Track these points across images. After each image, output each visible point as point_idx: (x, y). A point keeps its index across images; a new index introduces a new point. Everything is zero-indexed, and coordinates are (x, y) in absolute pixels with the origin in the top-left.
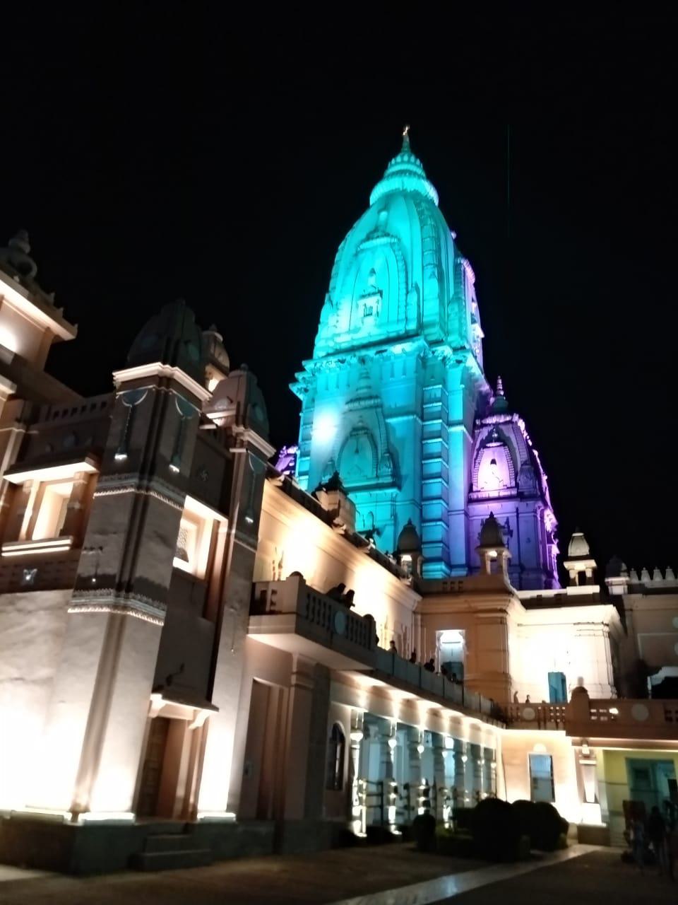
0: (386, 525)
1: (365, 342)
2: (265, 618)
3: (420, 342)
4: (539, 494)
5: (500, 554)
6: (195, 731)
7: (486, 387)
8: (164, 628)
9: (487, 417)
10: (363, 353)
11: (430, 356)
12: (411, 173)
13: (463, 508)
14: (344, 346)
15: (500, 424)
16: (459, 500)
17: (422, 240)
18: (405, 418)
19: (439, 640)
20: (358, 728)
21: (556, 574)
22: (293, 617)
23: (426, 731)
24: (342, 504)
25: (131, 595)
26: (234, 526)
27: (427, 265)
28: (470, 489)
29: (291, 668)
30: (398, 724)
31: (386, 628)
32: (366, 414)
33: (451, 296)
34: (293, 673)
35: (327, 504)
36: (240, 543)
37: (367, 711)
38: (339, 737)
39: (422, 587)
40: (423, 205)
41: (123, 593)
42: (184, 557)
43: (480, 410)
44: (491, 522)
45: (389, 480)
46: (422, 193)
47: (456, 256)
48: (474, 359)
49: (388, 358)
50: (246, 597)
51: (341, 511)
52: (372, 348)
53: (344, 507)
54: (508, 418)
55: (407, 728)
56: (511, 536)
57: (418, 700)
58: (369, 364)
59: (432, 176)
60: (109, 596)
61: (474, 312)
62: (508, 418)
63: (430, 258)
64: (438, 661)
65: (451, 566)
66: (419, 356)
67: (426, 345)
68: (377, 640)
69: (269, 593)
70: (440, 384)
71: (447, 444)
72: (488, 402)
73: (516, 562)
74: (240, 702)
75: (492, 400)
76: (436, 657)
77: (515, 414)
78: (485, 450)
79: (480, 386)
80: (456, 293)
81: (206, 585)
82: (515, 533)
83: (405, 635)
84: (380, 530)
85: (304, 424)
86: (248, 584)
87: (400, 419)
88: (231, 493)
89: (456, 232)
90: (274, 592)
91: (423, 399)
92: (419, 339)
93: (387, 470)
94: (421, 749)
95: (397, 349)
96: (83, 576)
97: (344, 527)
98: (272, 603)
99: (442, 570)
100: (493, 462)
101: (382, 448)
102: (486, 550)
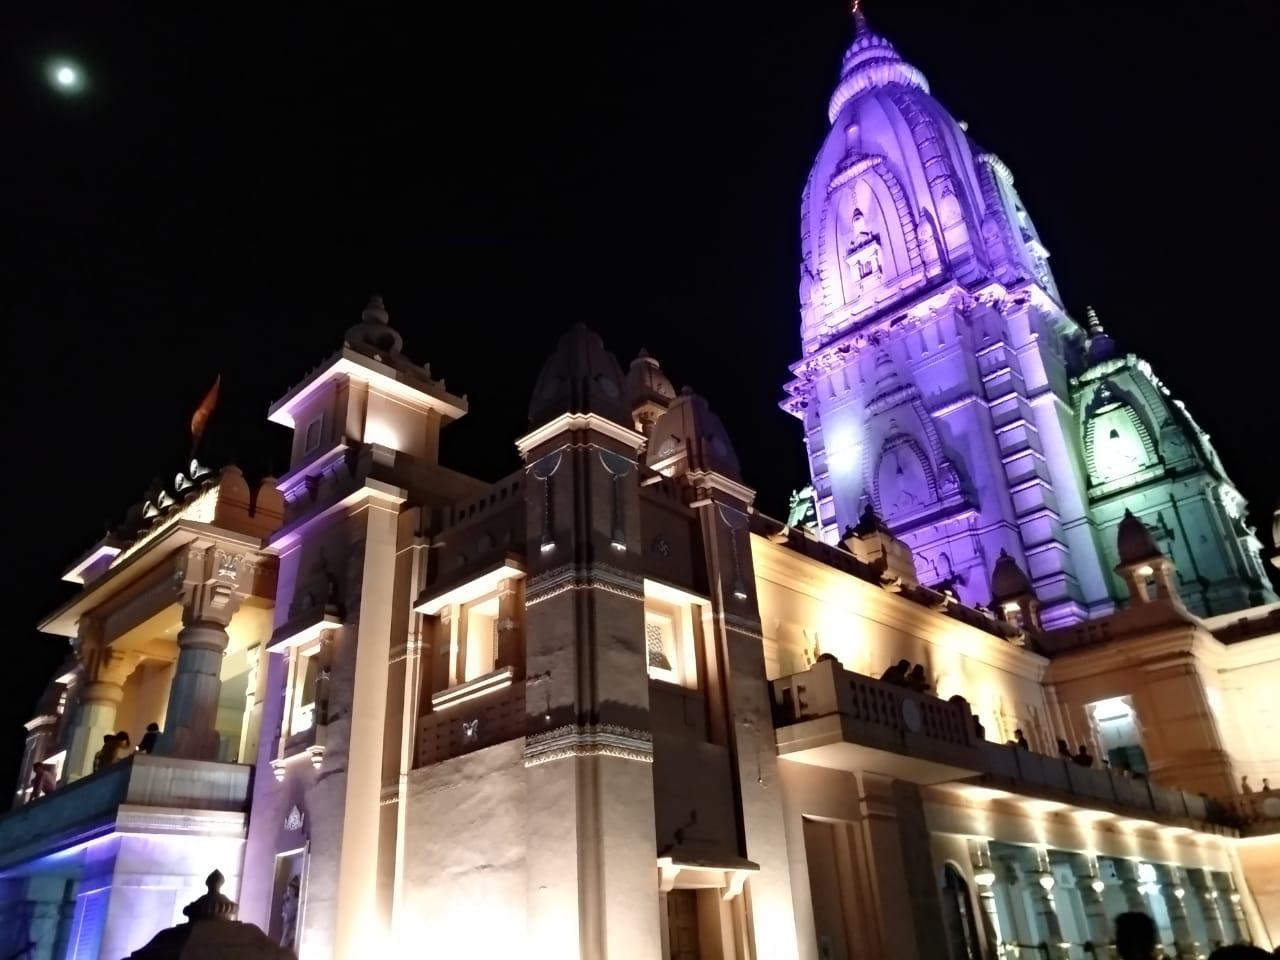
0: (970, 567)
1: (871, 312)
2: (797, 728)
3: (954, 289)
4: (1202, 464)
5: (1157, 569)
6: (733, 902)
7: (1072, 328)
8: (656, 767)
9: (1085, 370)
10: (873, 329)
11: (974, 305)
12: (877, 61)
13: (1084, 515)
14: (843, 326)
15: (1109, 375)
16: (1074, 503)
17: (918, 146)
18: (960, 404)
19: (1092, 718)
20: (985, 867)
21: (1266, 581)
22: (837, 719)
23: (1100, 858)
24: (888, 550)
25: (599, 727)
27: (934, 180)
28: (1089, 485)
29: (857, 793)
30: (1050, 852)
31: (1002, 714)
32: (898, 414)
33: (982, 212)
34: (862, 800)
35: (866, 556)
36: (737, 630)
37: (992, 839)
39: (1045, 644)
41: (588, 727)
42: (664, 664)
43: (1072, 362)
44: (1130, 525)
45: (958, 500)
46: (902, 82)
47: (975, 154)
48: (1041, 292)
49: (912, 326)
50: (764, 704)
51: (889, 560)
52: (883, 319)
53: (892, 553)
54: (1120, 364)
55: (1065, 856)
56: (1173, 538)
57: (1073, 811)
59: (909, 57)
60: (570, 735)
61: (1023, 224)
62: (1120, 364)
63: (936, 169)
64: (1098, 747)
65: (1086, 605)
66: (956, 309)
67: (963, 291)
68: (980, 730)
69: (795, 691)
70: (999, 341)
71: (1035, 426)
73: (1190, 575)
74: (789, 853)
75: (1088, 344)
76: (1095, 744)
77: (1129, 355)
78: (1096, 420)
79: (1064, 328)
80: (988, 207)
81: (702, 696)
82: (1178, 533)
83: (1036, 719)
84: (964, 577)
85: (813, 452)
86: (760, 683)
87: (952, 408)
88: (710, 568)
90: (801, 689)
91: (980, 372)
93: (950, 487)
94: (1098, 886)
95: (920, 311)
96: (534, 715)
97: (899, 582)
98: (803, 706)
99: (1073, 614)
100: (1114, 434)
102: (1133, 567)
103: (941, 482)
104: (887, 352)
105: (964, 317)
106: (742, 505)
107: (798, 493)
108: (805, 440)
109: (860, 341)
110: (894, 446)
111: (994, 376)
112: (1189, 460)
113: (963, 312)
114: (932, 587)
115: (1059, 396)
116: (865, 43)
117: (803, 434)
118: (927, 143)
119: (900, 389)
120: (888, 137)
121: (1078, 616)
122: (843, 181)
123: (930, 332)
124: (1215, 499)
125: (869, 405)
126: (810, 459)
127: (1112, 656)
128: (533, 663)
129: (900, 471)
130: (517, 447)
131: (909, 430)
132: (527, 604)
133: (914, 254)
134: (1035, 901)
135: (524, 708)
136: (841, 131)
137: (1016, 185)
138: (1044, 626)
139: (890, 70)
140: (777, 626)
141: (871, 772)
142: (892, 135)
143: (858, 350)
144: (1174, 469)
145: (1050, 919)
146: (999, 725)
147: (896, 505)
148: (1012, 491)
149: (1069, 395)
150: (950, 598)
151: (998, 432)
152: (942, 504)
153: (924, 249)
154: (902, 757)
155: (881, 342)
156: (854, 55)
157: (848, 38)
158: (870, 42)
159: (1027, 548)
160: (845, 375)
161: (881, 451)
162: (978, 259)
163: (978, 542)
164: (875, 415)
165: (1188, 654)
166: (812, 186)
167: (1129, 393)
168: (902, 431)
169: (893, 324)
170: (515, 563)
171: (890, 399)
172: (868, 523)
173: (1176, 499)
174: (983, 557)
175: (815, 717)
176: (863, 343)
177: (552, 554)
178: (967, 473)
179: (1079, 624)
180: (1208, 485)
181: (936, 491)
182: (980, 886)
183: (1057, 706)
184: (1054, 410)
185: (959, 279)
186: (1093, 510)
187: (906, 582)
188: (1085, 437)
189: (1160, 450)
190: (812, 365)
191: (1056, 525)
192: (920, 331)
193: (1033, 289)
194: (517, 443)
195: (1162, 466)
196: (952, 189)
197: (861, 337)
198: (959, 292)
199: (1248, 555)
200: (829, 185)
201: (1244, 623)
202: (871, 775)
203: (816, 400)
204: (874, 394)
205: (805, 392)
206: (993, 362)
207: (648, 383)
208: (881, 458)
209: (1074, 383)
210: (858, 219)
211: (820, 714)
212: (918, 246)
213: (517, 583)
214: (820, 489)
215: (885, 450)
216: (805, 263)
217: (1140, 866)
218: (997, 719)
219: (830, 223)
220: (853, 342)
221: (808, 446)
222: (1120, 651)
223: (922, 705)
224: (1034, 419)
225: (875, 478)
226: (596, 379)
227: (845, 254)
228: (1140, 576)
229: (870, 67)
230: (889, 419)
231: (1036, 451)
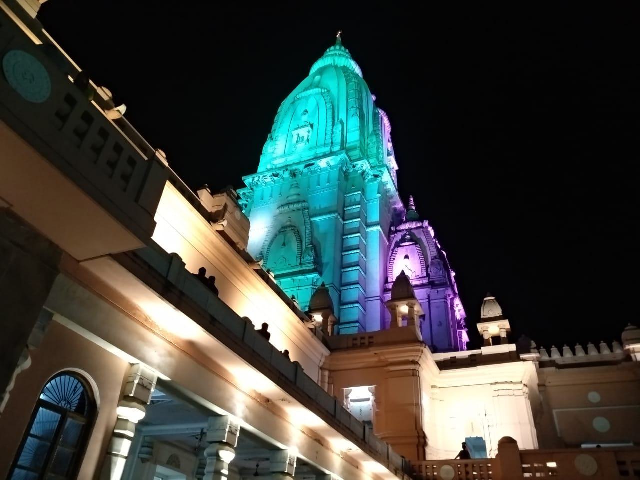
13: (379, 295)
15: (412, 229)
18: (328, 216)
32: (294, 215)
33: (370, 133)
49: (316, 172)
54: (419, 225)
58: (299, 177)
62: (419, 225)
63: (353, 102)
66: (341, 169)
77: (425, 221)
78: (398, 249)
80: (375, 131)
87: (324, 217)
93: (309, 258)
95: (323, 164)
100: (407, 257)
101: (306, 241)
103: (305, 255)
104: (298, 182)
109: (285, 172)
110: (285, 231)
111: (351, 208)
113: (345, 173)
118: (352, 91)
119: (299, 202)
120: (335, 85)
122: (303, 96)
123: (324, 176)
125: (279, 207)
129: (284, 245)
133: (329, 137)
137: (391, 134)
143: (283, 178)
144: (434, 282)
147: (276, 263)
148: (343, 271)
149: (389, 234)
151: (345, 237)
153: (335, 137)
155: (297, 177)
159: (342, 303)
160: (272, 190)
161: (278, 232)
162: (361, 150)
164: (281, 214)
165: (416, 363)
167: (420, 239)
168: (293, 225)
171: (292, 207)
173: (431, 299)
176: (287, 175)
178: (321, 254)
180: (450, 295)
181: (301, 259)
184: (378, 236)
186: (385, 295)
188: (392, 255)
189: (429, 270)
190: (256, 179)
191: (361, 295)
192: (319, 176)
195: (428, 278)
197: (287, 170)
198: (346, 159)
201: (454, 359)
204: (283, 203)
205: (249, 197)
206: (353, 201)
209: (393, 229)
210: (305, 114)
212: (332, 134)
219: (290, 114)
220: (281, 172)
224: (366, 238)
225: (270, 244)
228: (400, 313)
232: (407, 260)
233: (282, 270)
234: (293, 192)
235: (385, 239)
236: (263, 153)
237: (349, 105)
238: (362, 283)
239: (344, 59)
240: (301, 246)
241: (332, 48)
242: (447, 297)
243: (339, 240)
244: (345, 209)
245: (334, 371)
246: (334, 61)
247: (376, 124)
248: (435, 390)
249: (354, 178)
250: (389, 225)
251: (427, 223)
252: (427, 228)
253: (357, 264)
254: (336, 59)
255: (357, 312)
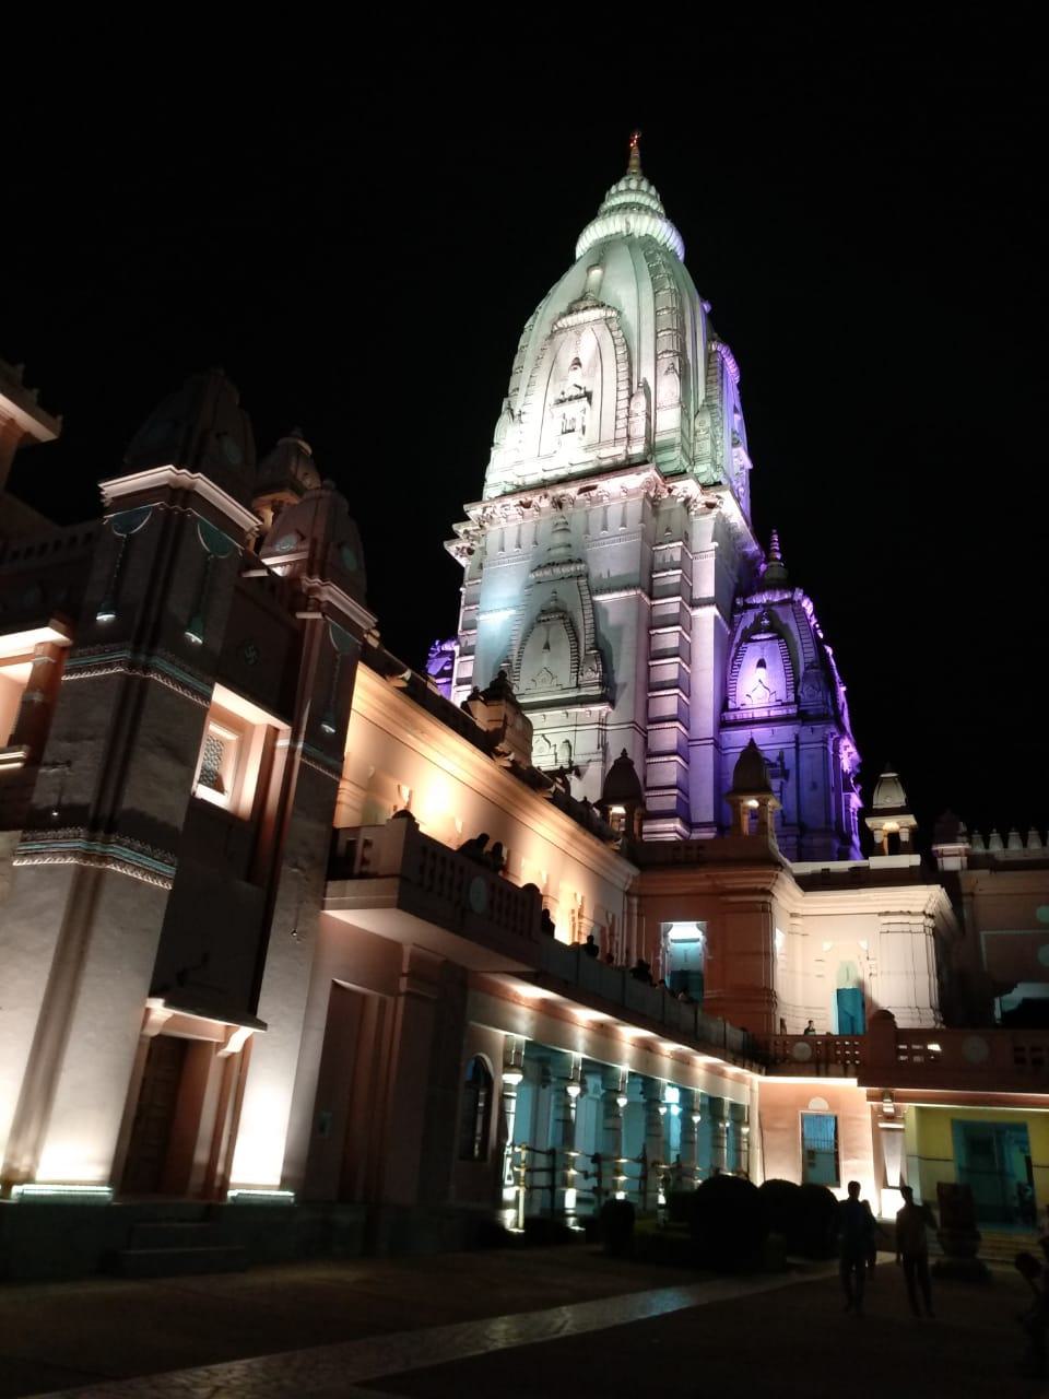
0: (590, 761)
1: (563, 473)
2: (351, 885)
4: (832, 713)
6: (229, 1059)
7: (754, 548)
10: (560, 491)
12: (640, 207)
13: (712, 736)
14: (530, 480)
15: (773, 604)
16: (705, 721)
18: (624, 594)
19: (666, 936)
21: (856, 839)
22: (396, 882)
23: (631, 1074)
24: (509, 722)
26: (302, 737)
27: (662, 353)
31: (580, 916)
32: (561, 588)
33: (700, 403)
34: (403, 975)
35: (485, 723)
38: (484, 1079)
39: (642, 855)
40: (659, 258)
41: (101, 834)
45: (596, 691)
46: (659, 240)
47: (710, 339)
49: (599, 500)
52: (572, 483)
54: (786, 596)
55: (599, 1067)
57: (617, 1024)
58: (568, 508)
63: (667, 342)
65: (690, 824)
66: (647, 494)
69: (360, 845)
71: (689, 635)
72: (757, 571)
73: (793, 818)
75: (763, 567)
77: (797, 589)
78: (749, 644)
79: (744, 545)
80: (708, 398)
82: (793, 775)
83: (612, 928)
84: (580, 768)
85: (467, 604)
86: (323, 828)
87: (616, 595)
89: (711, 303)
90: (367, 844)
91: (652, 567)
92: (648, 469)
94: (622, 1102)
95: (610, 486)
96: (40, 807)
97: (511, 757)
98: (365, 862)
100: (761, 664)
101: (586, 640)
102: (741, 797)
104: (567, 519)
105: (653, 506)
106: (356, 630)
107: (441, 644)
108: (461, 589)
109: (543, 500)
112: (822, 706)
113: (653, 500)
114: (546, 772)
115: (720, 612)
116: (633, 185)
117: (460, 582)
118: (665, 312)
119: (570, 562)
120: (630, 292)
121: (681, 836)
124: (834, 750)
125: (535, 570)
126: (462, 611)
127: (698, 880)
128: (56, 747)
129: (547, 647)
130: (101, 490)
131: (569, 609)
132: (64, 678)
133: (621, 424)
134: (557, 1107)
135: (29, 799)
136: (584, 270)
138: (644, 836)
139: (650, 222)
140: (371, 774)
141: (424, 949)
142: (635, 290)
143: (539, 510)
144: (806, 711)
145: (568, 1129)
146: (574, 926)
147: (533, 680)
148: (650, 695)
150: (558, 786)
152: (580, 691)
154: (457, 938)
156: (619, 193)
157: (618, 173)
158: (639, 185)
160: (519, 531)
162: (683, 450)
163: (604, 738)
165: (769, 893)
166: (539, 317)
167: (787, 625)
168: (559, 605)
169: (582, 491)
170: (62, 626)
171: (557, 570)
172: (498, 690)
174: (605, 753)
175: (375, 876)
176: (545, 504)
177: (109, 624)
179: (677, 842)
180: (832, 734)
182: (505, 1084)
183: (635, 917)
185: (658, 465)
187: (519, 759)
188: (735, 658)
189: (799, 690)
190: (489, 511)
191: (682, 737)
192: (605, 509)
193: (727, 495)
194: (101, 485)
196: (678, 368)
197: (546, 496)
199: (847, 811)
200: (555, 324)
202: (424, 952)
203: (484, 550)
207: (293, 469)
208: (533, 629)
210: (575, 369)
211: (381, 873)
213: (59, 651)
214: (463, 645)
215: (539, 622)
216: (509, 399)
217: (668, 1089)
218: (573, 919)
219: (546, 364)
220: (535, 499)
221: (463, 597)
222: (708, 877)
223: (492, 887)
226: (218, 436)
227: (553, 402)
229: (632, 212)
230: (551, 589)
231: (683, 660)
232: (761, 670)
233: (546, 693)
234: (559, 538)
235: (725, 625)
236: (495, 441)
237: (659, 345)
238: (683, 717)
239: (647, 218)
240: (578, 652)
241: (622, 186)
242: (827, 739)
243: (644, 638)
244: (654, 576)
245: (646, 896)
246: (628, 223)
247: (712, 382)
248: (797, 921)
249: (671, 511)
250: (732, 595)
251: (800, 594)
252: (800, 602)
253: (674, 685)
254: (631, 218)
255: (675, 769)
